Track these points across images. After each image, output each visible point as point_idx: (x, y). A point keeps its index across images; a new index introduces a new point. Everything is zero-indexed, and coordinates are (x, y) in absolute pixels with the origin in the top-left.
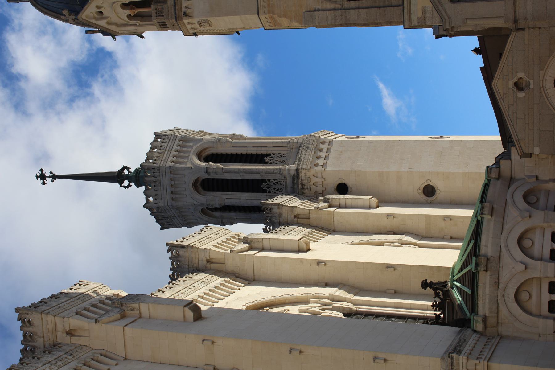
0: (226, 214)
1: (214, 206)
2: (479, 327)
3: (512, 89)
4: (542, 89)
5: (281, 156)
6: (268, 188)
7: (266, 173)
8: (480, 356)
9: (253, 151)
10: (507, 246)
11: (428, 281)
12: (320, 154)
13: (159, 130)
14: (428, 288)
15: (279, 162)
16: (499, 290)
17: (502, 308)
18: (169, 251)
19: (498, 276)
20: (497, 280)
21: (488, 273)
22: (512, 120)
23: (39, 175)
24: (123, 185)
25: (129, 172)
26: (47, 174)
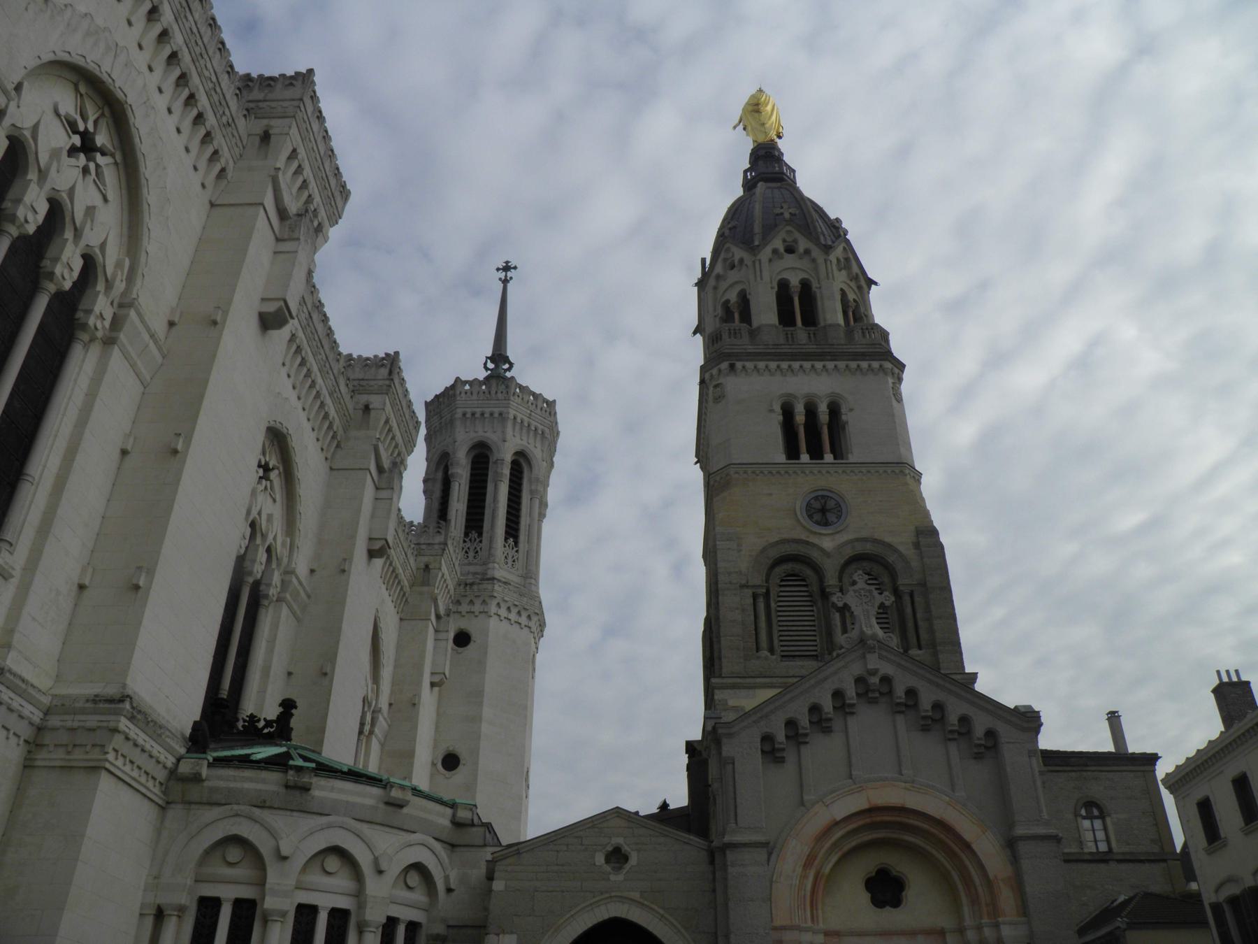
0: (438, 488)
1: (450, 467)
2: (185, 768)
3: (609, 843)
4: (607, 895)
5: (514, 561)
6: (470, 540)
7: (491, 537)
8: (119, 756)
9: (524, 521)
10: (330, 826)
11: (294, 711)
12: (514, 611)
13: (558, 408)
14: (281, 709)
15: (506, 557)
16: (248, 807)
17: (216, 812)
18: (387, 355)
19: (276, 806)
20: (268, 804)
21: (282, 790)
22: (555, 843)
23: (509, 264)
24: (489, 361)
25: (506, 370)
26: (509, 274)
